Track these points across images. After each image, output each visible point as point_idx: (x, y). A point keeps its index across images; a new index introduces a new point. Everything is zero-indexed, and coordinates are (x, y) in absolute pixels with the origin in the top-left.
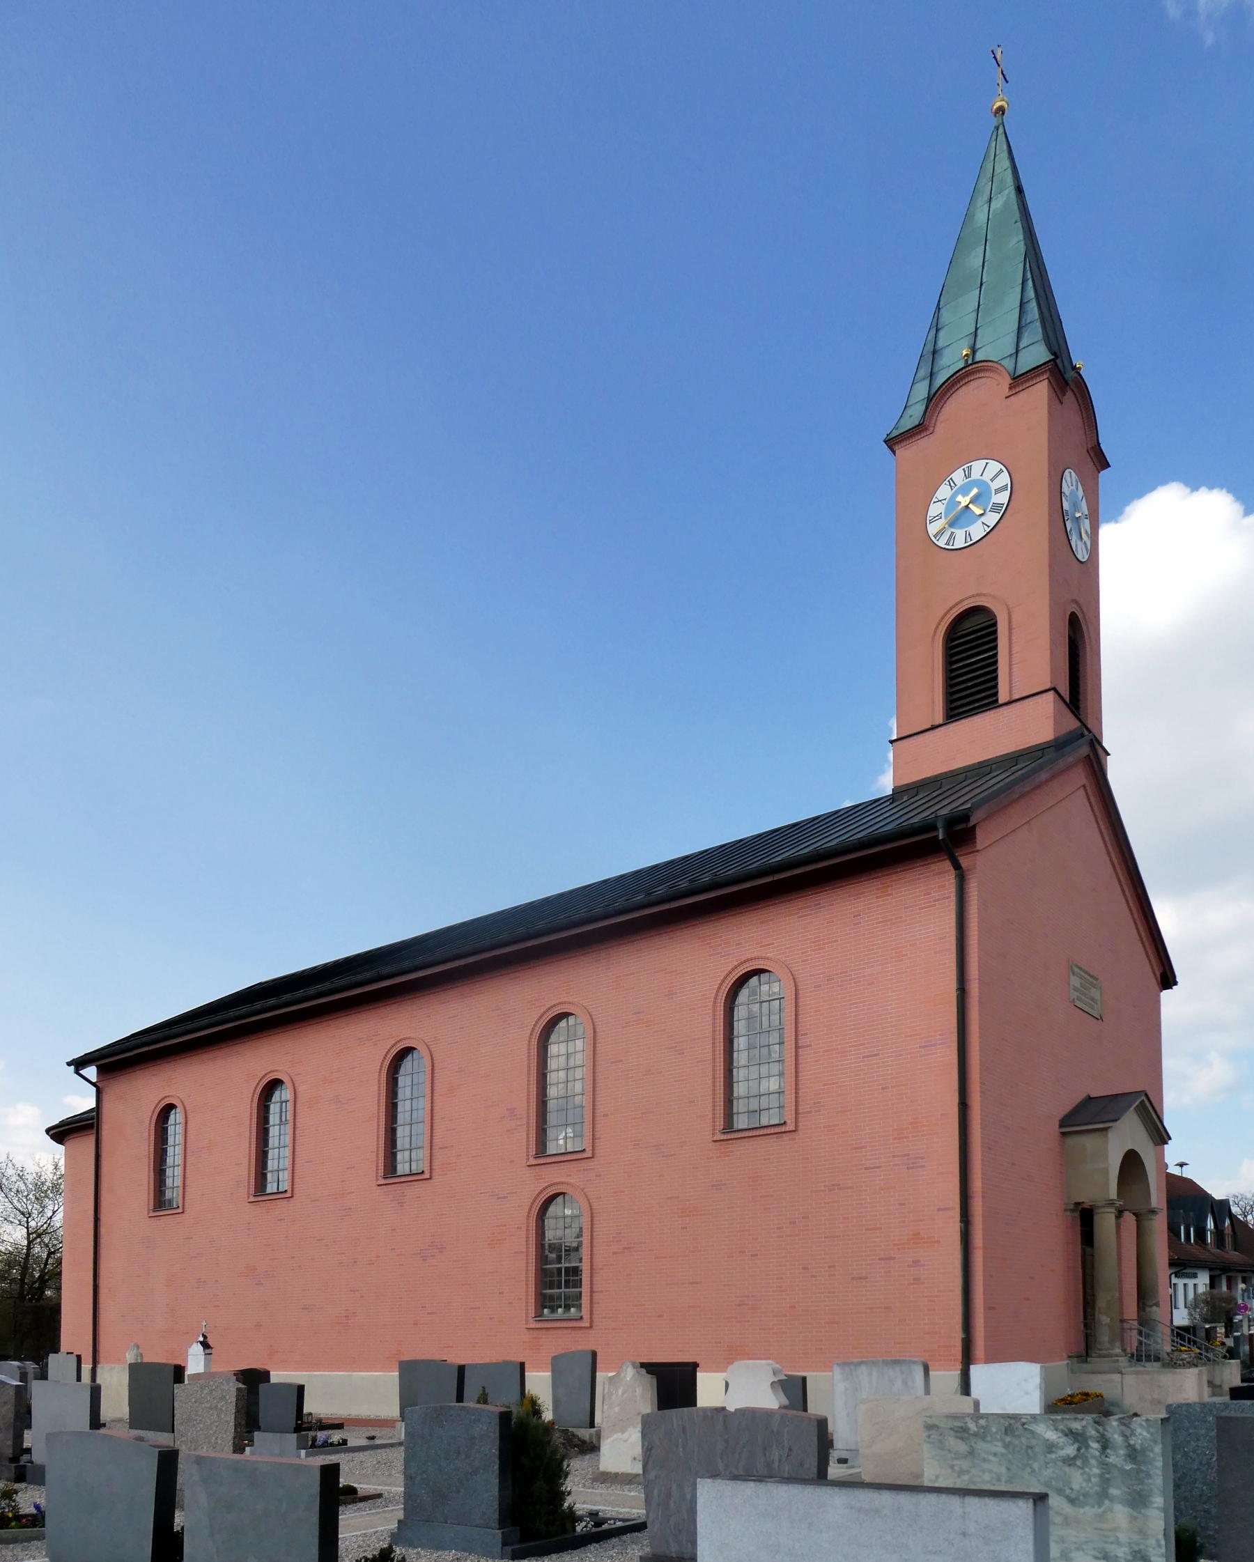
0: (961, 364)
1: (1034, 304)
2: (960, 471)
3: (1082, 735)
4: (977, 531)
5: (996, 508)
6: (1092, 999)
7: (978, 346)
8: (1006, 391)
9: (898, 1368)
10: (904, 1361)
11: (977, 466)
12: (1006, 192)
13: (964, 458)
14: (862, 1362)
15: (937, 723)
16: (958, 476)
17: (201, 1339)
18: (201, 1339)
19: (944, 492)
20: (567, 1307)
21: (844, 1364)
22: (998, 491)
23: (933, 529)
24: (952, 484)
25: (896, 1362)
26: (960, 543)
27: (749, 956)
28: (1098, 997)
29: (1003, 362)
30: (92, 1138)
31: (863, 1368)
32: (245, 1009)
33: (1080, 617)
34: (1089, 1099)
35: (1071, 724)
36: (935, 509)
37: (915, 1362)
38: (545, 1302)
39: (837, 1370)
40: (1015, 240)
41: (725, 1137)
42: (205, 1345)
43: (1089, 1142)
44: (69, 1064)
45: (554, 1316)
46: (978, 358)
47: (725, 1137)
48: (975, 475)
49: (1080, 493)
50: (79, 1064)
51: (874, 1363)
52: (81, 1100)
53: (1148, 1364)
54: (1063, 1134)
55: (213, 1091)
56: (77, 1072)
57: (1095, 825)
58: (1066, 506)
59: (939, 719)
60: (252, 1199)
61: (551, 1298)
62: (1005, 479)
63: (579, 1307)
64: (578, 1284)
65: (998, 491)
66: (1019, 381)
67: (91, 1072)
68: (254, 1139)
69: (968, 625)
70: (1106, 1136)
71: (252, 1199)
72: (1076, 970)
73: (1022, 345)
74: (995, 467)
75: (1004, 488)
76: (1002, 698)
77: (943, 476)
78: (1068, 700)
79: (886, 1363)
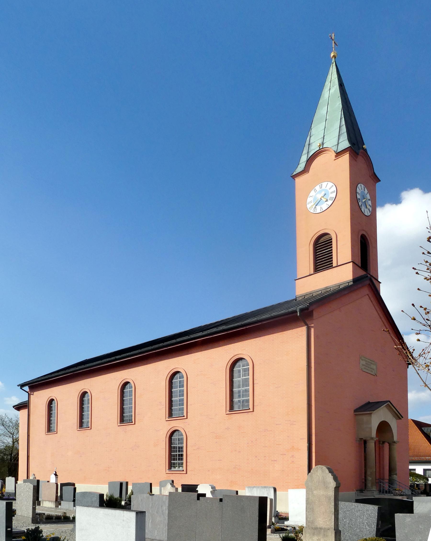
0: (318, 149)
1: (344, 127)
2: (318, 186)
3: (367, 277)
4: (325, 207)
5: (331, 198)
6: (371, 368)
7: (324, 142)
8: (334, 158)
9: (266, 489)
10: (268, 487)
11: (324, 184)
12: (335, 87)
13: (319, 181)
14: (254, 487)
15: (311, 274)
16: (317, 188)
17: (55, 473)
18: (55, 473)
19: (312, 193)
20: (179, 467)
21: (249, 487)
22: (332, 193)
23: (309, 206)
24: (315, 191)
25: (265, 487)
26: (319, 211)
27: (237, 353)
28: (374, 367)
29: (333, 148)
30: (27, 410)
31: (255, 488)
32: (83, 367)
33: (367, 236)
34: (369, 403)
35: (362, 273)
36: (309, 200)
37: (270, 487)
38: (171, 466)
39: (247, 489)
40: (338, 104)
41: (230, 413)
42: (56, 475)
43: (365, 418)
44: (18, 386)
45: (179, 469)
46: (324, 147)
47: (230, 413)
48: (324, 187)
49: (366, 191)
50: (22, 386)
51: (258, 487)
52: (24, 397)
53: (386, 494)
54: (356, 415)
55: (66, 395)
56: (21, 388)
57: (373, 308)
58: (359, 197)
59: (312, 272)
60: (47, 434)
61: (174, 464)
62: (334, 188)
63: (182, 467)
64: (182, 459)
65: (332, 193)
66: (339, 154)
67: (27, 388)
68: (79, 411)
69: (322, 240)
70: (371, 416)
71: (78, 429)
72: (363, 358)
73: (340, 141)
74: (330, 184)
75: (334, 192)
76: (334, 264)
77: (312, 188)
78: (360, 265)
79: (262, 487)
